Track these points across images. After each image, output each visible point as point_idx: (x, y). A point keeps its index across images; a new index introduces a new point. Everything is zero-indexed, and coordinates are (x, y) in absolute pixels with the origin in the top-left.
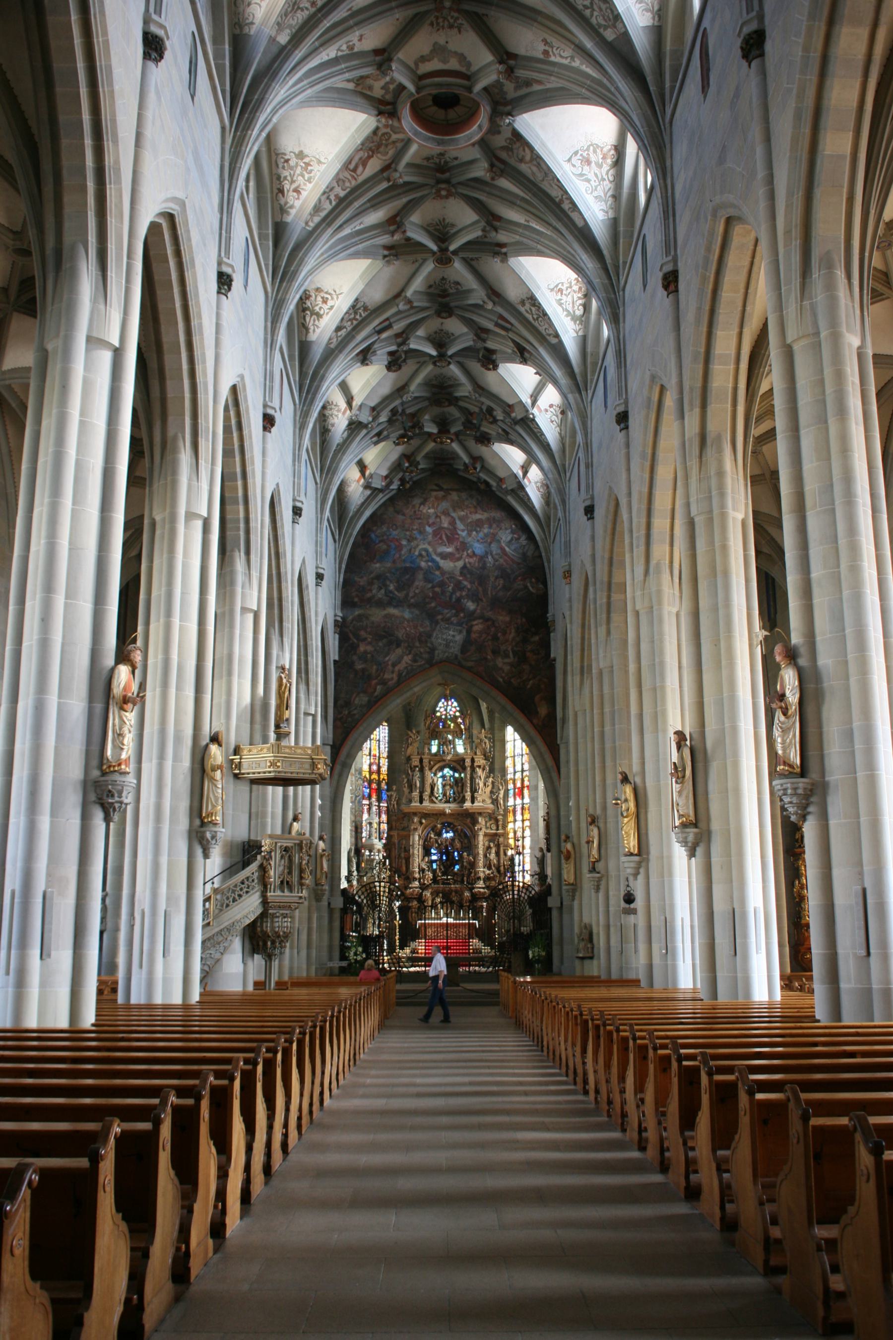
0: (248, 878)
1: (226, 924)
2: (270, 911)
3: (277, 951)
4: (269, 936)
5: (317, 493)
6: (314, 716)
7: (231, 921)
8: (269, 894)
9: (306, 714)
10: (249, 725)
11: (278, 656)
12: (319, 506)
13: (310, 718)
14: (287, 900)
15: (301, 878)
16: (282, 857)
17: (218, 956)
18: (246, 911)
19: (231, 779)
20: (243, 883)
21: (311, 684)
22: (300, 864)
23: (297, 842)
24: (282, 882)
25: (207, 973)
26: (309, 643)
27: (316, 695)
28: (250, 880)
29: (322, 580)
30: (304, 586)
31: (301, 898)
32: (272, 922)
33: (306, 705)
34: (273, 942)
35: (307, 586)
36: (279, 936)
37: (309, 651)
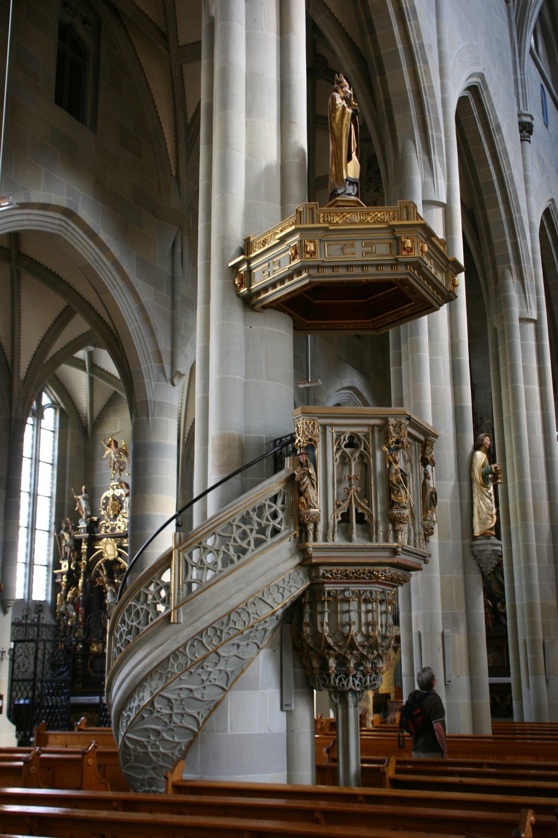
0: (260, 510)
1: (208, 619)
2: (328, 588)
3: (352, 683)
4: (329, 647)
5: (509, 16)
6: (537, 323)
7: (221, 611)
8: (311, 544)
9: (524, 320)
10: (278, 206)
11: (424, 185)
12: (515, 32)
13: (531, 326)
14: (361, 557)
15: (391, 504)
16: (344, 461)
17: (212, 694)
18: (258, 585)
19: (237, 310)
20: (246, 520)
21: (526, 276)
22: (387, 472)
23: (377, 422)
24: (346, 517)
25: (195, 734)
26: (515, 215)
27: (538, 293)
28: (267, 513)
29: (530, 132)
30: (493, 126)
31: (395, 552)
32: (334, 613)
33: (521, 306)
34: (342, 661)
35: (498, 127)
36: (352, 646)
37: (517, 228)
